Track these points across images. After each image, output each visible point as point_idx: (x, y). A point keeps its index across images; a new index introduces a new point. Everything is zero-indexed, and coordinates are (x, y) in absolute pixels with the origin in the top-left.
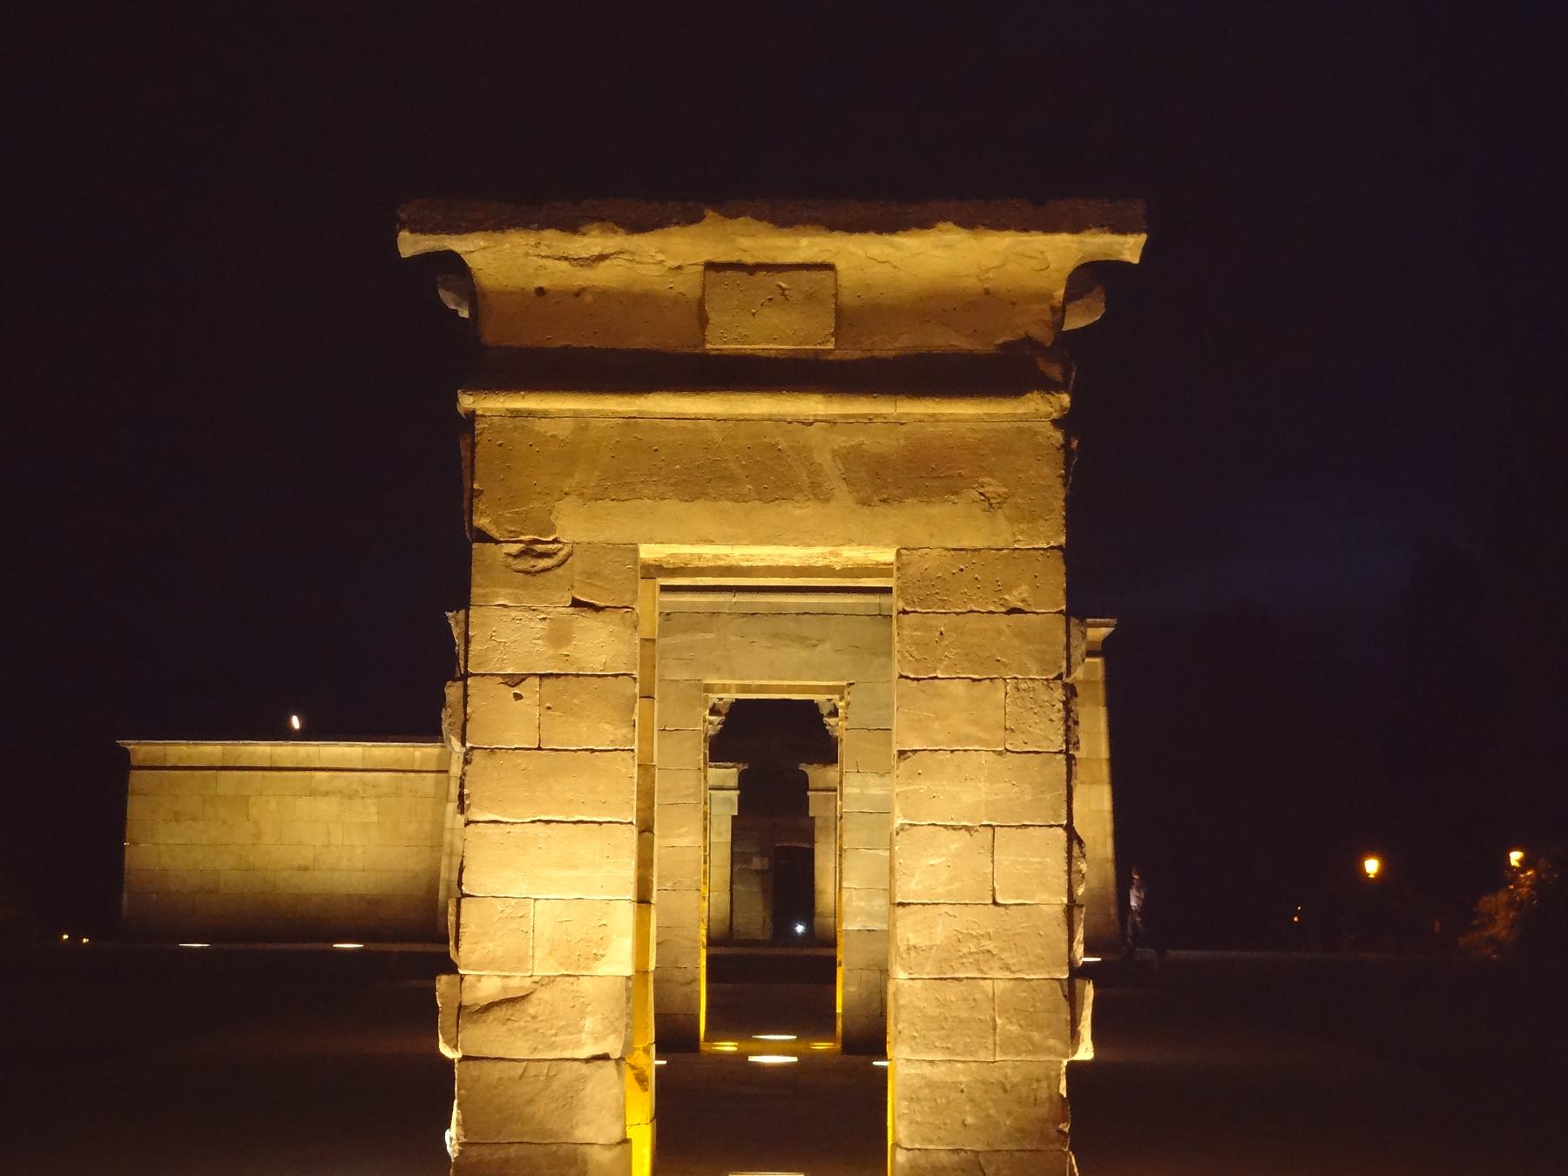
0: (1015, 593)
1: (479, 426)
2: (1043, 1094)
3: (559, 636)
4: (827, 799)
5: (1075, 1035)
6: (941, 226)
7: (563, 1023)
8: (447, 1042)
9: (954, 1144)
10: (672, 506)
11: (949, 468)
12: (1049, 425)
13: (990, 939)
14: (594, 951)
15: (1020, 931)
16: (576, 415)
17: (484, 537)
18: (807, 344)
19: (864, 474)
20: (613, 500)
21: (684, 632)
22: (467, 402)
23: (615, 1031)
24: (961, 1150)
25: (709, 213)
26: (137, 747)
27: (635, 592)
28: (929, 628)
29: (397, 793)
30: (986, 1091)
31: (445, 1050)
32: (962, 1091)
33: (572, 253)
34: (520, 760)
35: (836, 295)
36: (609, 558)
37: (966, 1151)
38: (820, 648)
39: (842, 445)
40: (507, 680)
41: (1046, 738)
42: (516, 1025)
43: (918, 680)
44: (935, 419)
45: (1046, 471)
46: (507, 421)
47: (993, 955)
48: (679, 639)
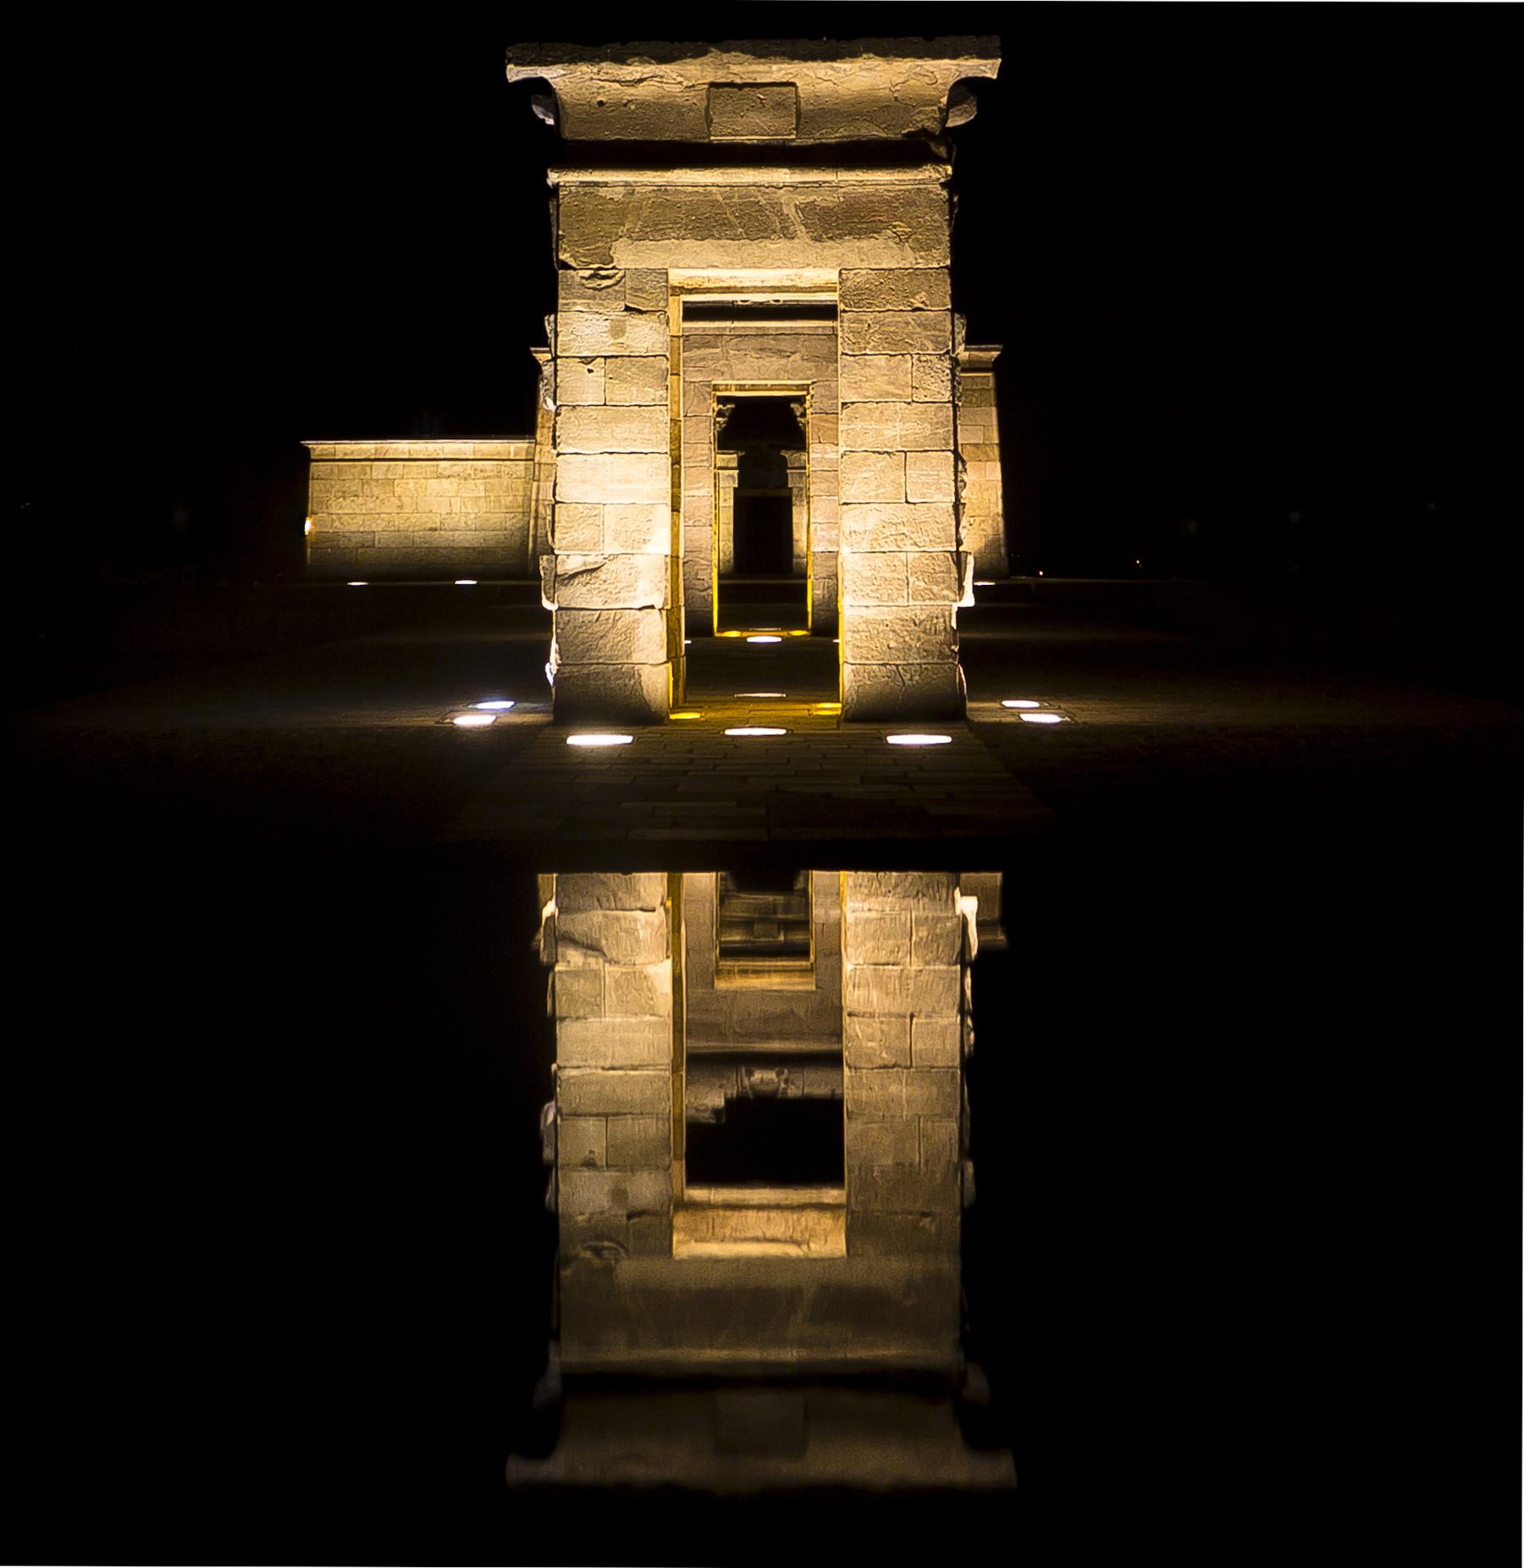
0: (917, 297)
2: (941, 626)
3: (618, 331)
5: (961, 588)
6: (865, 56)
7: (624, 584)
8: (548, 599)
9: (883, 659)
10: (690, 244)
11: (873, 216)
12: (940, 188)
13: (904, 525)
14: (644, 537)
15: (924, 520)
16: (627, 184)
17: (566, 266)
18: (777, 135)
19: (817, 220)
20: (651, 240)
21: (698, 348)
22: (553, 177)
23: (658, 589)
24: (888, 664)
25: (713, 49)
26: (315, 446)
27: (667, 300)
29: (499, 477)
30: (903, 625)
31: (546, 604)
32: (887, 625)
33: (621, 78)
34: (593, 413)
35: (797, 103)
36: (649, 278)
37: (890, 665)
38: (790, 359)
39: (802, 201)
40: (583, 360)
41: (939, 393)
42: (593, 586)
43: (854, 356)
44: (862, 184)
46: (580, 189)
47: (906, 536)
48: (694, 353)
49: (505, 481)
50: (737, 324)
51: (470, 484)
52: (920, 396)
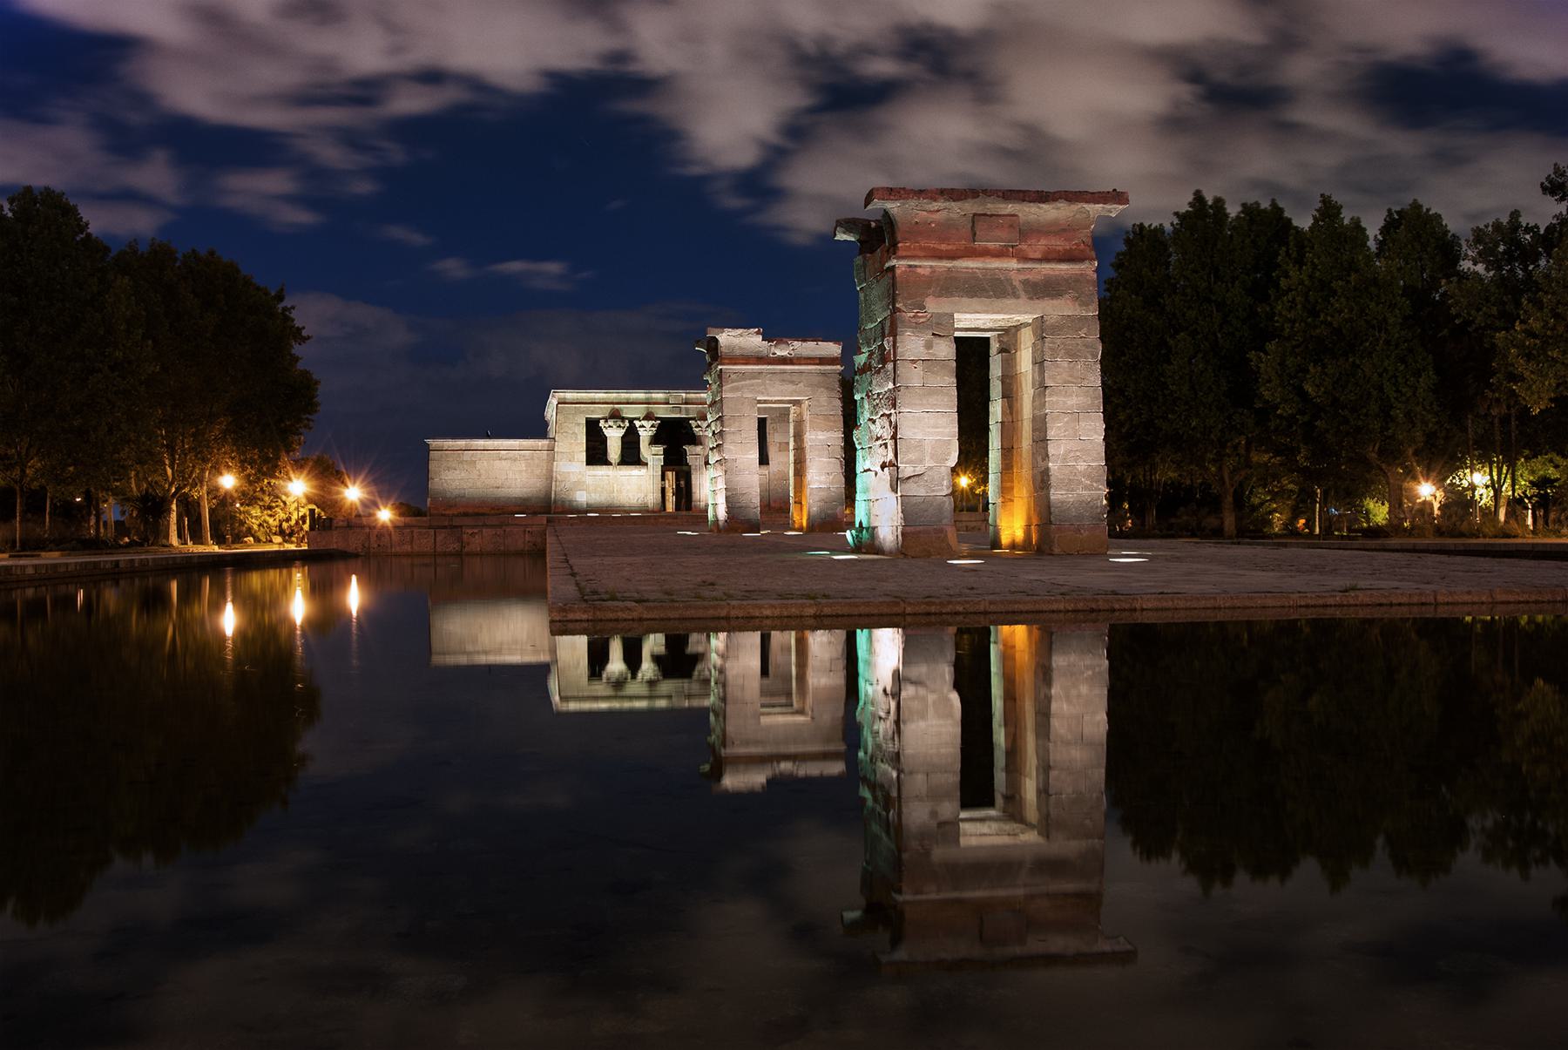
1: (898, 272)
2: (1099, 504)
3: (929, 346)
4: (696, 458)
10: (964, 299)
16: (931, 267)
17: (899, 310)
21: (750, 379)
28: (1054, 343)
29: (532, 459)
45: (1091, 288)
46: (908, 270)
48: (748, 382)
49: (536, 461)
50: (770, 367)
51: (518, 463)
52: (1085, 383)
